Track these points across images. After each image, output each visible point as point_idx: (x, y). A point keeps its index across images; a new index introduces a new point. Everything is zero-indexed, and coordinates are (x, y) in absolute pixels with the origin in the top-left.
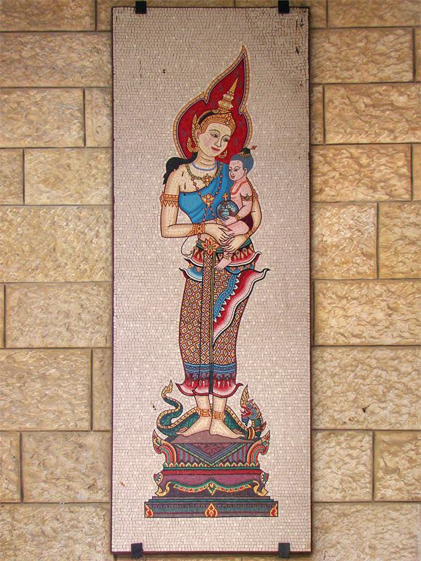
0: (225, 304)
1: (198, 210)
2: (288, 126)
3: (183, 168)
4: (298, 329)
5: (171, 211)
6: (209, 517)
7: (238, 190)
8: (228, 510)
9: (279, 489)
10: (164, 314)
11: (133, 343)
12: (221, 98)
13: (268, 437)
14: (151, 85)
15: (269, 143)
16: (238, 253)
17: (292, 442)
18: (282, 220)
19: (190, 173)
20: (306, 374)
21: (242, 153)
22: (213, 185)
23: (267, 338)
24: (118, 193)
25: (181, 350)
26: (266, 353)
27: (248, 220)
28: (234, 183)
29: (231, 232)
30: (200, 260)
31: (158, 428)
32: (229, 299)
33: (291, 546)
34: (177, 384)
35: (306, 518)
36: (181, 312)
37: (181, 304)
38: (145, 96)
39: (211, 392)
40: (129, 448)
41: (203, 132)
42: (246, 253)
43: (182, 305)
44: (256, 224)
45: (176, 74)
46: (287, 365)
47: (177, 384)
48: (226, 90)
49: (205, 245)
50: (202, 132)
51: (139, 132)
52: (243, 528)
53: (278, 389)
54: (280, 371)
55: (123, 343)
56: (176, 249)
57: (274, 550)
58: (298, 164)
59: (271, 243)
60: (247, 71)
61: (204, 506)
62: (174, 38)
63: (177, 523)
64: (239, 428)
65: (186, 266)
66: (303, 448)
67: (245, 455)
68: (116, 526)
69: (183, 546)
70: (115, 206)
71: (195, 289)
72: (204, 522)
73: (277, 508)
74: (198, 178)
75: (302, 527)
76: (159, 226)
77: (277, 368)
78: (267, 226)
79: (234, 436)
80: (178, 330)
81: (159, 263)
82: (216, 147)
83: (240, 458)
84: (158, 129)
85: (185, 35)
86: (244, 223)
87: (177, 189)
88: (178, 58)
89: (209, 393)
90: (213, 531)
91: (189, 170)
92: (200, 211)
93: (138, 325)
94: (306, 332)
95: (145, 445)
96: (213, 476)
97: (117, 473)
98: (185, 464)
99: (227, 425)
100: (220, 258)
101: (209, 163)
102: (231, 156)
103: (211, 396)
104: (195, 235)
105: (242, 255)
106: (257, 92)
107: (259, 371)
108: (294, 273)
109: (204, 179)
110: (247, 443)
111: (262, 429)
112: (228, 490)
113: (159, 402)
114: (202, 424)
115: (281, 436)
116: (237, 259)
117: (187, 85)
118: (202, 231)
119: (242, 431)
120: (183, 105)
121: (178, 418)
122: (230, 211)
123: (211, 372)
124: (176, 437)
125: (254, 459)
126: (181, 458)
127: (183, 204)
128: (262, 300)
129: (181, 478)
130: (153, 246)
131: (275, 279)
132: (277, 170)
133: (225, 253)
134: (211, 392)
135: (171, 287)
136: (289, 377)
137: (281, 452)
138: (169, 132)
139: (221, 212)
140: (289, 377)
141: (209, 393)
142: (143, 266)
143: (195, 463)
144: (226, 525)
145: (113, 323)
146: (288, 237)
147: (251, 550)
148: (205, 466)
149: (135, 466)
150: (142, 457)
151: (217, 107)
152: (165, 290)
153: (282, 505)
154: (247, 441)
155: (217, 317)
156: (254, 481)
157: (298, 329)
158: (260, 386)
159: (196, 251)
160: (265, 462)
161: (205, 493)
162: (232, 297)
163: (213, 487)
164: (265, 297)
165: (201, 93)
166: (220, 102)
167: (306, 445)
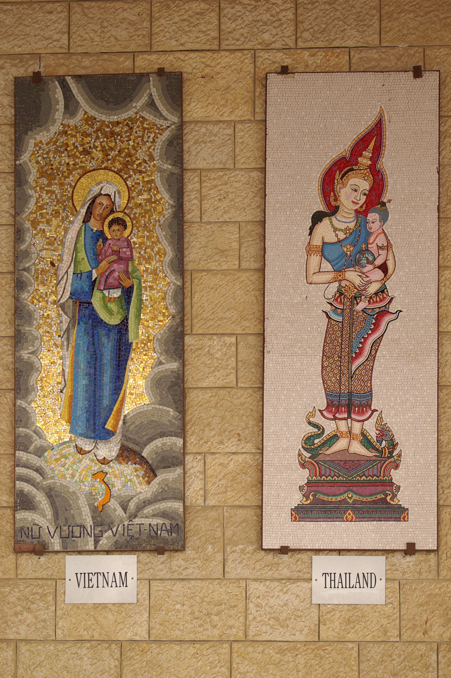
0: (363, 341)
1: (341, 258)
2: (419, 181)
3: (326, 221)
4: (427, 362)
5: (315, 259)
6: (347, 521)
7: (374, 240)
8: (365, 515)
10: (308, 350)
11: (281, 375)
12: (361, 155)
13: (399, 455)
14: (299, 144)
15: (402, 197)
16: (374, 297)
17: (421, 459)
18: (414, 268)
19: (332, 225)
22: (354, 234)
23: (400, 371)
24: (269, 244)
25: (323, 381)
26: (398, 383)
27: (384, 268)
28: (369, 234)
29: (368, 279)
30: (341, 303)
31: (303, 447)
32: (366, 336)
34: (319, 410)
35: (433, 522)
36: (324, 348)
37: (323, 341)
38: (294, 154)
39: (349, 417)
40: (278, 464)
41: (344, 186)
42: (381, 297)
43: (325, 342)
44: (390, 271)
45: (321, 133)
46: (417, 393)
47: (319, 410)
49: (345, 290)
51: (288, 187)
52: (378, 530)
53: (409, 415)
54: (411, 399)
55: (273, 375)
56: (320, 293)
58: (428, 217)
59: (403, 288)
60: (384, 130)
62: (320, 100)
63: (319, 526)
64: (374, 448)
65: (328, 308)
68: (266, 528)
69: (325, 545)
70: (266, 256)
71: (336, 328)
72: (343, 526)
74: (340, 230)
75: (429, 530)
76: (305, 274)
77: (408, 396)
78: (401, 273)
80: (321, 363)
81: (305, 306)
82: (355, 201)
84: (305, 185)
85: (330, 98)
86: (380, 271)
87: (321, 239)
88: (323, 118)
89: (348, 418)
90: (351, 533)
91: (331, 222)
93: (285, 360)
95: (291, 462)
96: (351, 488)
98: (327, 477)
100: (358, 301)
101: (349, 216)
102: (369, 209)
103: (349, 420)
104: (336, 281)
105: (378, 299)
106: (392, 149)
107: (392, 399)
108: (424, 314)
109: (345, 231)
113: (304, 426)
114: (341, 444)
115: (411, 454)
117: (331, 144)
118: (342, 278)
119: (377, 450)
121: (320, 439)
122: (367, 259)
123: (350, 400)
125: (387, 473)
126: (323, 472)
128: (395, 337)
130: (299, 291)
131: (407, 319)
132: (410, 222)
133: (363, 297)
134: (349, 417)
135: (315, 327)
137: (411, 468)
138: (314, 187)
139: (359, 260)
140: (418, 404)
141: (348, 418)
142: (290, 309)
143: (335, 477)
144: (362, 528)
146: (419, 282)
149: (282, 480)
150: (289, 472)
152: (309, 329)
154: (381, 459)
155: (355, 353)
157: (427, 362)
158: (393, 412)
159: (337, 295)
162: (369, 335)
164: (397, 335)
165: (342, 150)
166: (360, 159)
167: (433, 462)
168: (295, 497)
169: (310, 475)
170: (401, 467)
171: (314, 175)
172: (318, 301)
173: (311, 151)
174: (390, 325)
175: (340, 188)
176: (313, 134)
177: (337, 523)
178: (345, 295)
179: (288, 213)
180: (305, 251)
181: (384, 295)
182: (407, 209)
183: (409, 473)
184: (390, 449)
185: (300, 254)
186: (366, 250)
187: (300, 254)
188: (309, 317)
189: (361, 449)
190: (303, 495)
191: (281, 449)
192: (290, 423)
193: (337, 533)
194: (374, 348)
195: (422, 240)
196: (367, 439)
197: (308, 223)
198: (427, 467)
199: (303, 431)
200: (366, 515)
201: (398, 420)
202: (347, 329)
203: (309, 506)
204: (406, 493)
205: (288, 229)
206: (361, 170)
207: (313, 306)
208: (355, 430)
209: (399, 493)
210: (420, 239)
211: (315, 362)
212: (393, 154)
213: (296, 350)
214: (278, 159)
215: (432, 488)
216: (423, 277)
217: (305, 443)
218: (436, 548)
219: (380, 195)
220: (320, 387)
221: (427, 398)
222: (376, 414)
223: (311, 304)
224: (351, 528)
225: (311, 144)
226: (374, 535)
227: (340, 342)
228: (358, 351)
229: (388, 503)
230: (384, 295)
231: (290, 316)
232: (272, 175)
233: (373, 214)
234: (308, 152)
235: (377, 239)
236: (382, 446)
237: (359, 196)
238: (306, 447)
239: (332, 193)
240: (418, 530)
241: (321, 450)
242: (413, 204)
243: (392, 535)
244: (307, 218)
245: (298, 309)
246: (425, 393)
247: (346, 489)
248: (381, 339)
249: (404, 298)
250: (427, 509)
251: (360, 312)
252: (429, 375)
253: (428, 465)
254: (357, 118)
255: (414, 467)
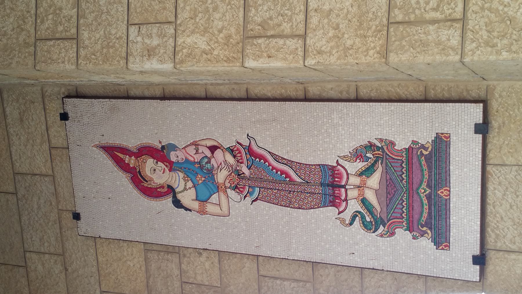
0: (275, 171)
3: (179, 196)
4: (291, 111)
5: (210, 208)
6: (449, 195)
9: (425, 131)
10: (284, 220)
11: (307, 246)
12: (128, 165)
13: (381, 140)
14: (124, 214)
17: (385, 119)
18: (211, 123)
20: (327, 106)
21: (165, 151)
22: (188, 174)
23: (300, 138)
24: (200, 245)
25: (312, 208)
26: (311, 139)
27: (213, 149)
28: (187, 160)
29: (223, 163)
30: (244, 188)
31: (374, 232)
32: (271, 167)
33: (478, 122)
35: (451, 107)
36: (283, 206)
38: (132, 219)
39: (344, 187)
40: (391, 257)
41: (152, 180)
42: (237, 152)
43: (277, 204)
44: (215, 144)
45: (116, 196)
46: (320, 122)
48: (123, 161)
49: (233, 184)
50: (153, 180)
51: (156, 226)
53: (340, 130)
54: (325, 128)
57: (481, 139)
59: (228, 132)
61: (440, 199)
64: (373, 165)
65: (249, 199)
66: (390, 109)
67: (396, 161)
68: (457, 275)
72: (454, 200)
73: (442, 134)
74: (185, 186)
75: (460, 112)
76: (222, 217)
77: (323, 131)
78: (216, 134)
79: (380, 169)
82: (162, 171)
83: (399, 165)
84: (154, 212)
86: (216, 152)
88: (105, 193)
89: (345, 188)
91: (180, 192)
92: (207, 184)
93: (294, 241)
94: (293, 105)
95: (389, 245)
97: (412, 270)
98: (404, 212)
99: (372, 174)
100: (241, 173)
102: (168, 160)
103: (347, 187)
104: (226, 191)
105: (239, 155)
107: (326, 146)
108: (249, 114)
109: (186, 181)
110: (386, 158)
111: (375, 145)
112: (426, 177)
113: (353, 230)
115: (379, 129)
116: (241, 159)
118: (223, 186)
119: (376, 162)
120: (135, 193)
121: (366, 215)
122: (207, 163)
123: (328, 185)
124: (381, 219)
126: (399, 215)
127: (204, 198)
128: (270, 141)
129: (416, 217)
130: (236, 224)
131: (254, 129)
132: (175, 125)
133: (238, 168)
135: (265, 212)
136: (330, 121)
137: (393, 129)
138: (155, 205)
139: (208, 170)
140: (330, 121)
141: (345, 188)
142: (251, 233)
143: (403, 204)
145: (293, 260)
147: (481, 159)
148: (405, 195)
150: (398, 248)
151: (134, 168)
153: (440, 129)
154: (385, 158)
155: (286, 178)
156: (419, 154)
158: (338, 145)
159: (237, 191)
160: (402, 144)
161: (429, 197)
163: (424, 190)
164: (268, 139)
165: (126, 179)
166: (131, 166)
168: (424, 245)
169: (402, 228)
170: (393, 140)
171: (146, 203)
172: (243, 208)
173: (129, 205)
174: (261, 145)
175: (154, 183)
176: (117, 203)
177: (451, 205)
178: (237, 184)
179: (176, 228)
180: (204, 216)
181: (235, 149)
182: (165, 128)
183: (398, 131)
184: (374, 149)
185: (206, 220)
186: (200, 164)
187: (206, 220)
188: (256, 217)
189: (375, 177)
190: (422, 236)
191: (376, 253)
192: (351, 242)
193: (462, 206)
194: (280, 161)
195: (188, 114)
196: (365, 171)
197: (182, 212)
198: (392, 114)
199: (358, 230)
200: (443, 175)
201: (346, 140)
202: (264, 184)
203: (433, 231)
204: (420, 135)
205: (187, 229)
206: (139, 165)
207: (248, 213)
208: (356, 182)
209: (420, 142)
210: (188, 117)
211: (295, 214)
212: (125, 138)
213: (285, 231)
214: (137, 232)
215: (414, 108)
216: (218, 114)
217: (370, 229)
218: (482, 105)
219: (156, 150)
220: (317, 212)
221: (325, 112)
222: (341, 162)
223: (246, 214)
224: (457, 192)
225: (124, 205)
226: (465, 170)
227: (276, 191)
228: (284, 175)
229: (431, 153)
230: (235, 149)
231: (257, 233)
232: (149, 238)
233: (171, 156)
234: (130, 207)
235: (191, 154)
236: (372, 157)
237: (159, 168)
238: (373, 229)
239: (158, 190)
240: (460, 123)
241: (377, 216)
242: (161, 122)
243: (466, 150)
244: (179, 212)
245: (250, 225)
246: (320, 114)
247: (415, 196)
248: (273, 154)
249: (237, 131)
250: (437, 114)
251: (251, 172)
252: (303, 110)
253: (390, 112)
254: (102, 166)
255: (393, 126)
